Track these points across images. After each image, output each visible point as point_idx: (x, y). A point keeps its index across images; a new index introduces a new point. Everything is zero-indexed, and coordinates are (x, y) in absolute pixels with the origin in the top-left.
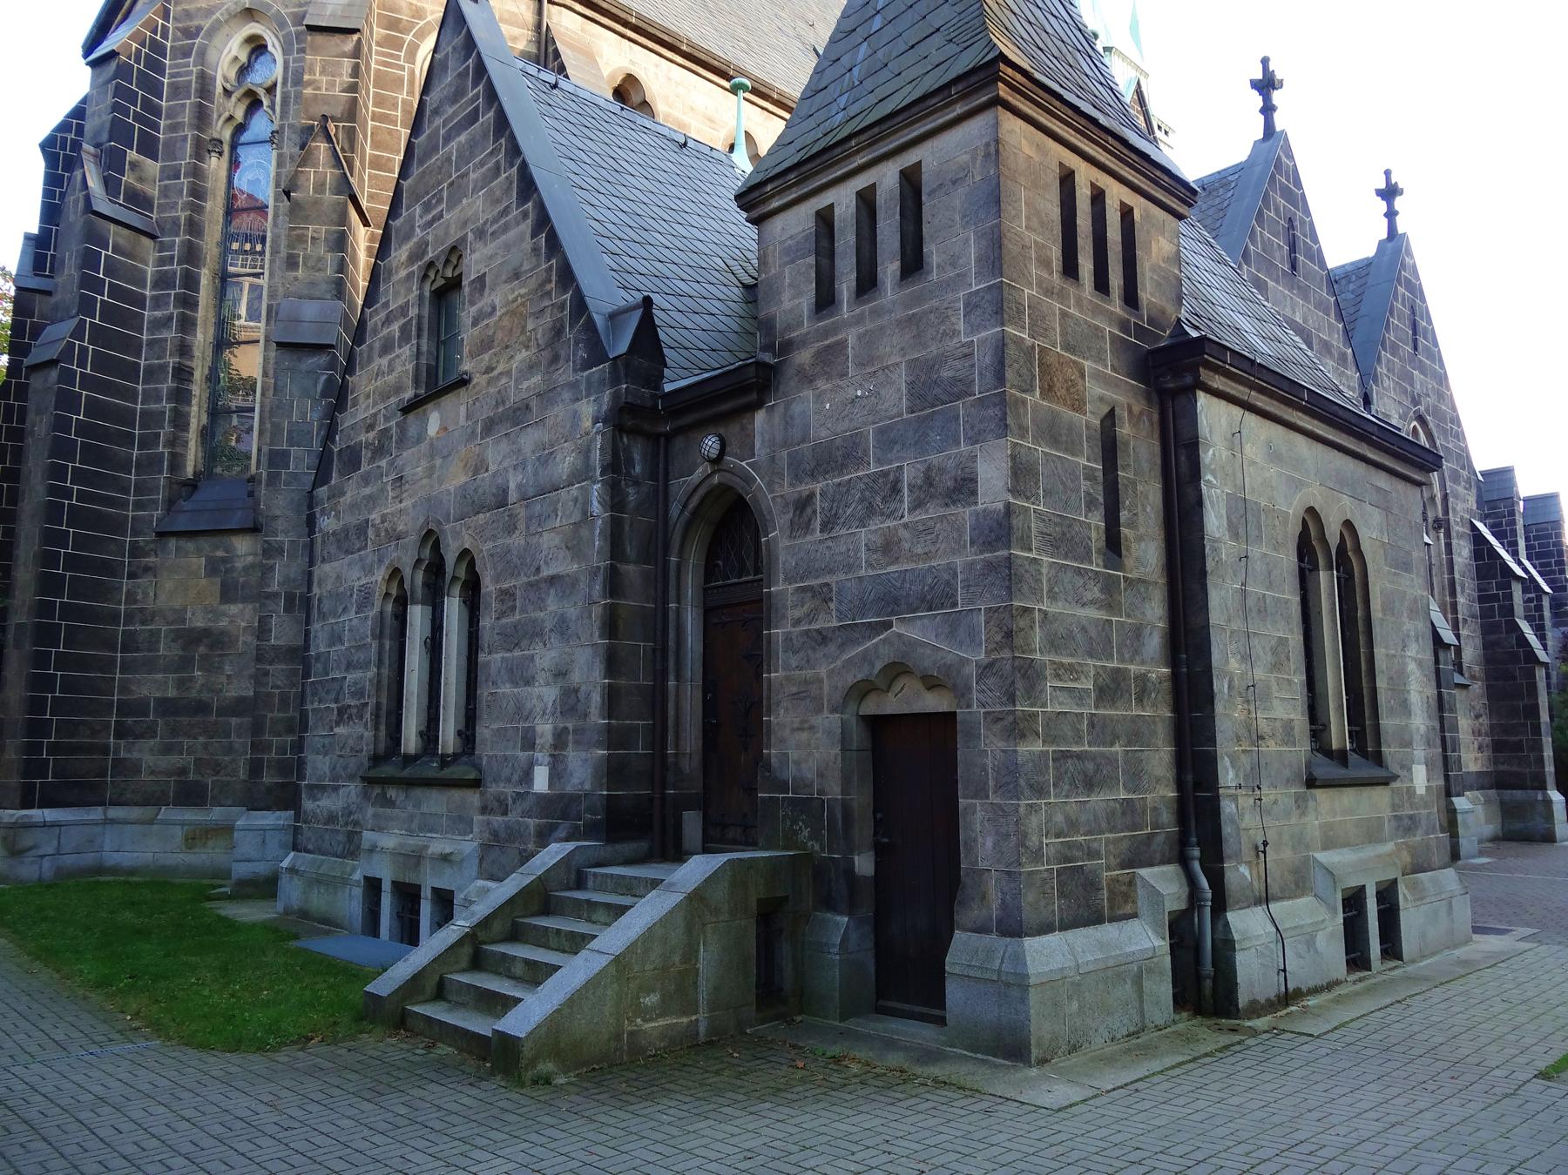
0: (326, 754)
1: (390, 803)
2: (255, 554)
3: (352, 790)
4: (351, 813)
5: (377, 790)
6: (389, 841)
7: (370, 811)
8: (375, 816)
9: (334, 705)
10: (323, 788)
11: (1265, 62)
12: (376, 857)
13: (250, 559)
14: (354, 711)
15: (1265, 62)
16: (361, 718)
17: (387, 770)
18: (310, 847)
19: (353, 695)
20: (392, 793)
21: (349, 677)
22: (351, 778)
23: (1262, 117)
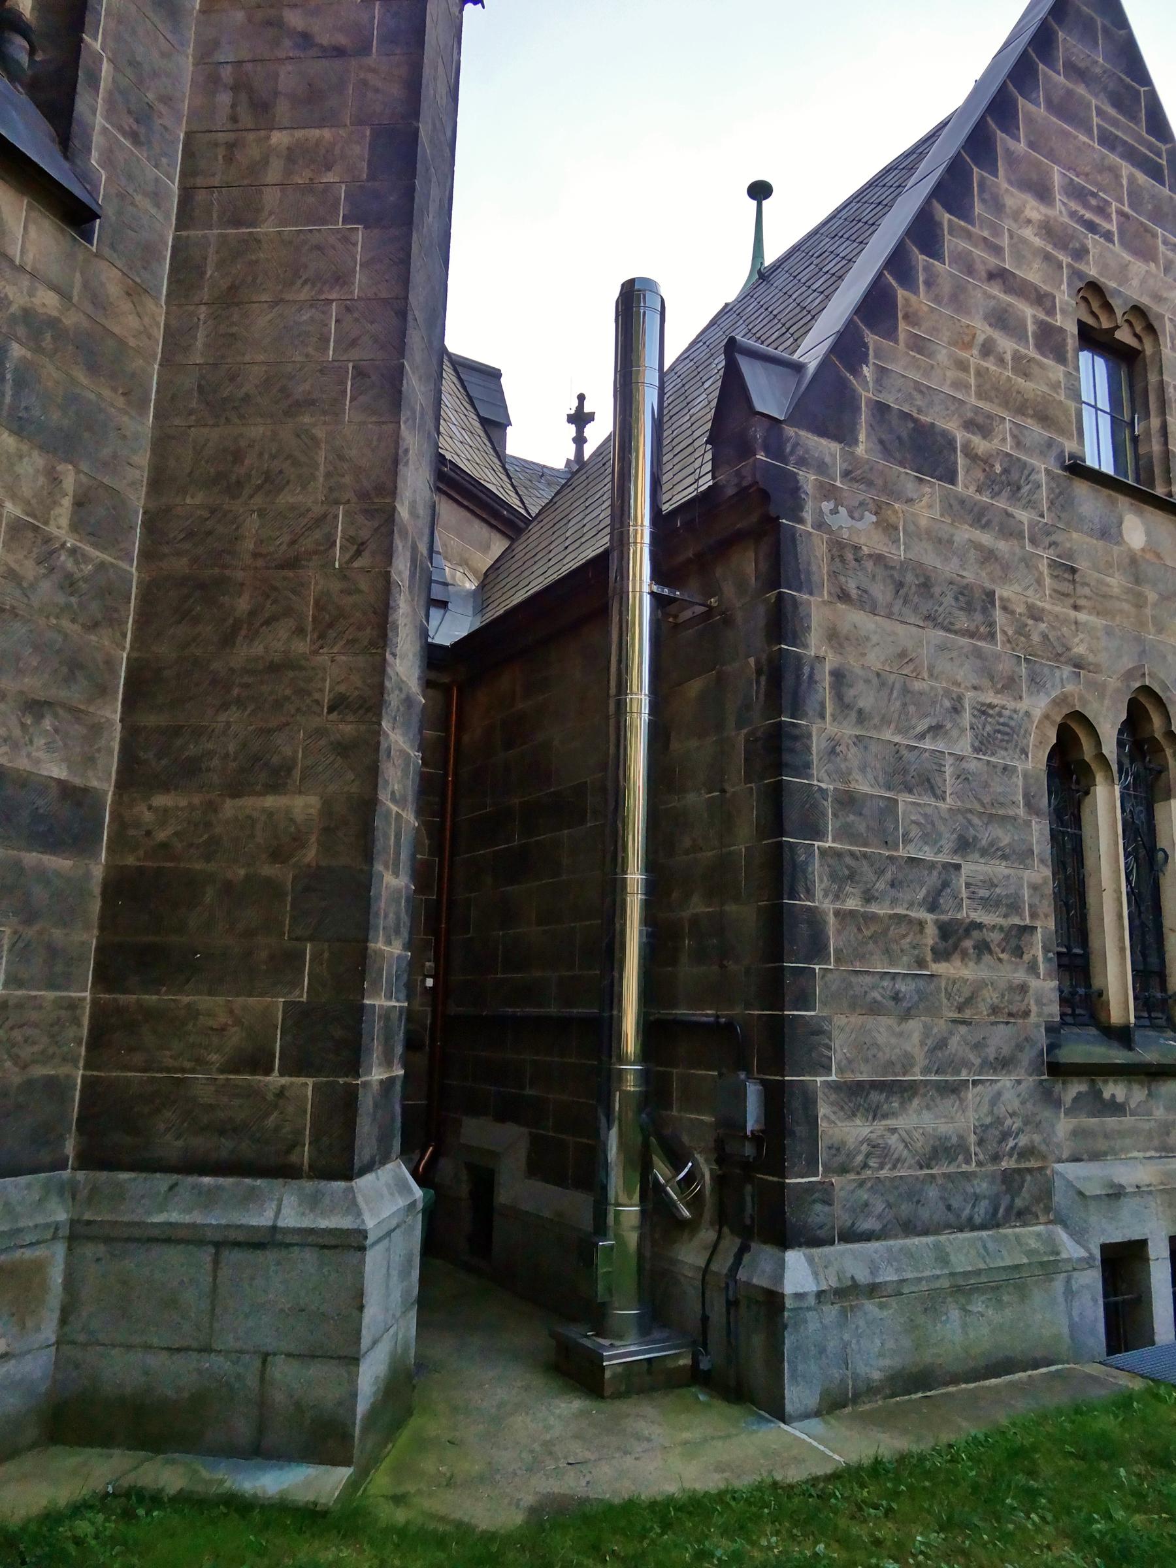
0: (907, 1015)
1: (1116, 1108)
2: (63, 294)
3: (1012, 1089)
4: (1005, 1136)
5: (1077, 1087)
6: (1135, 1171)
7: (1063, 1126)
8: (1075, 1133)
9: (922, 914)
10: (907, 1090)
11: (581, 398)
12: (1128, 1206)
13: (47, 301)
14: (995, 937)
15: (581, 398)
16: (1018, 952)
17: (1084, 1049)
18: (868, 1224)
19: (988, 904)
20: (1114, 1090)
21: (968, 868)
22: (1003, 1064)
23: (574, 446)
